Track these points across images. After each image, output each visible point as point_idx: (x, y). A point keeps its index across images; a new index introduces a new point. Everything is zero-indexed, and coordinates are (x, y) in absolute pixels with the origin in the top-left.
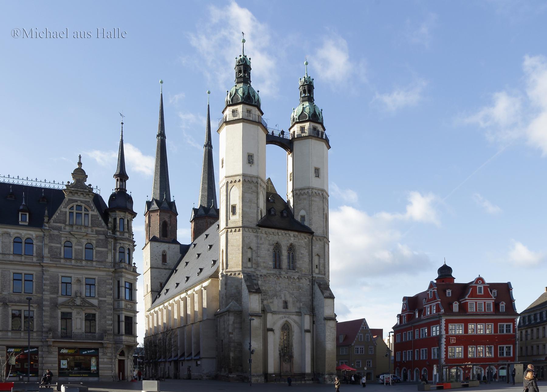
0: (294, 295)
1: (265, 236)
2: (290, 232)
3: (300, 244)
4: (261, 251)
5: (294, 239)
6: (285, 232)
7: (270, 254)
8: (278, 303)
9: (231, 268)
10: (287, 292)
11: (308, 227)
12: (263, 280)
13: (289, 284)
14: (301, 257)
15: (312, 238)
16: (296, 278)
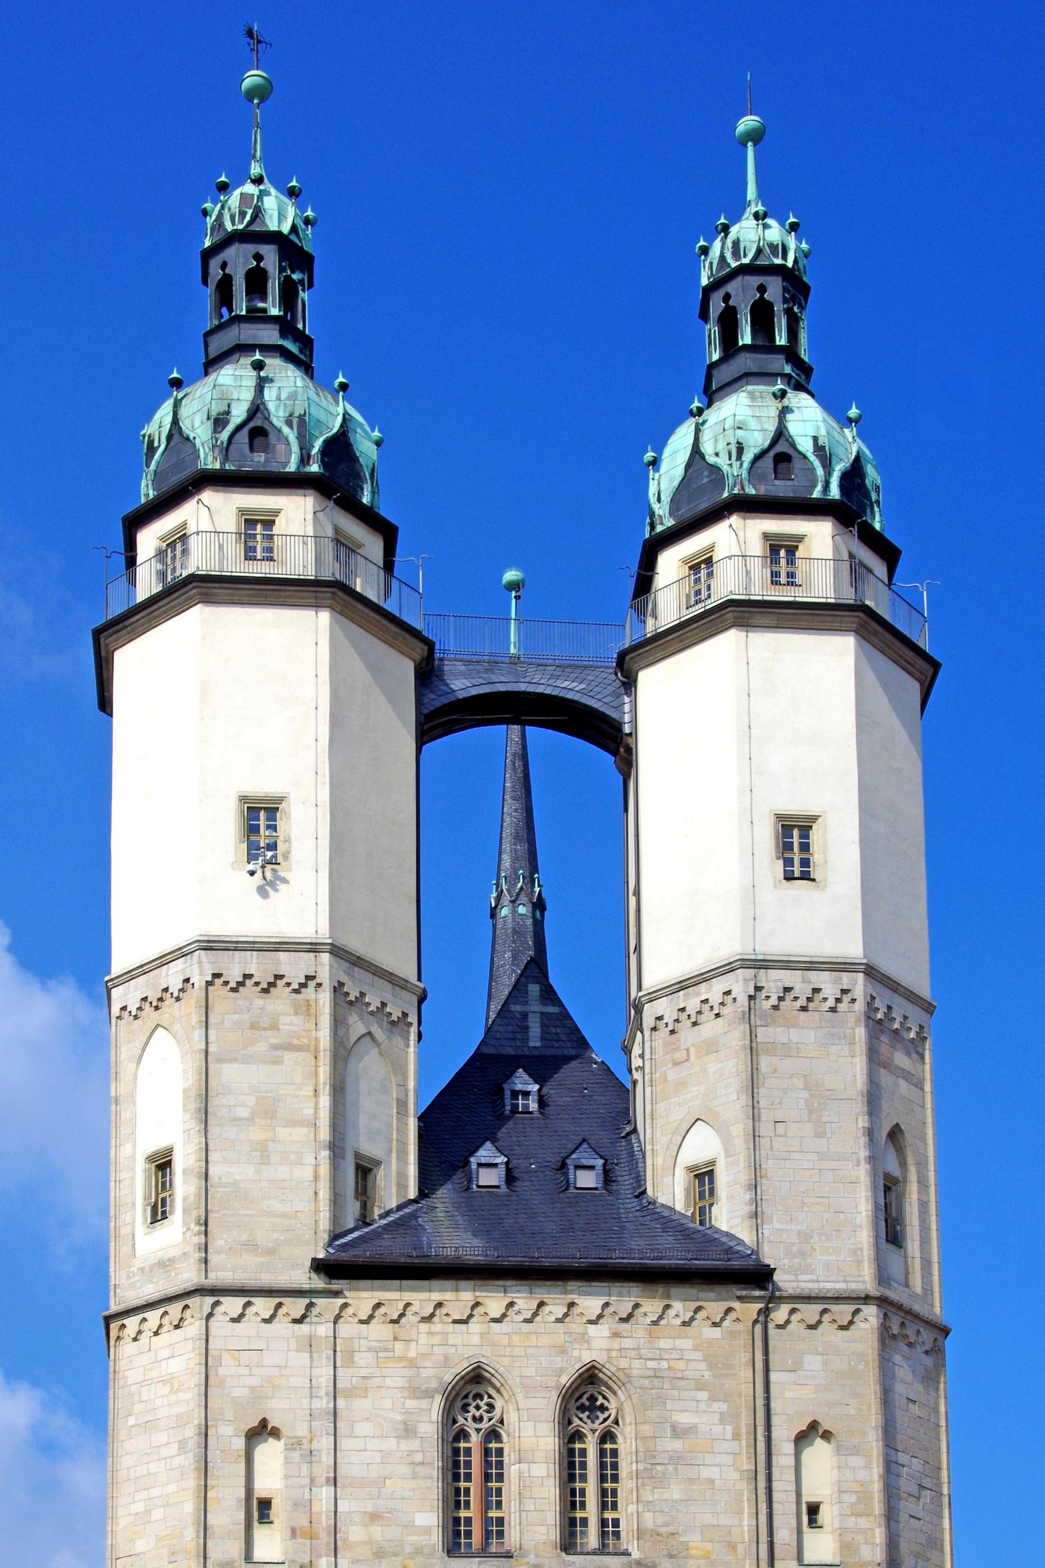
3: (664, 1364)
5: (616, 1335)
7: (419, 1458)
11: (733, 1237)
14: (676, 1459)
15: (765, 1312)
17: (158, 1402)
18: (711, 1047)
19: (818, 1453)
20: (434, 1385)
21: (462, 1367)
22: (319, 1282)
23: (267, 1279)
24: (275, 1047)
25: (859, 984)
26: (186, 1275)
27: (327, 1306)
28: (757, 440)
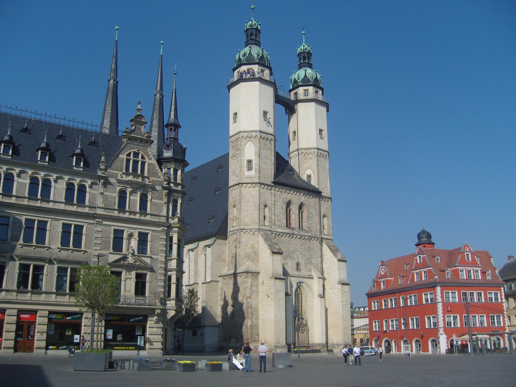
0: (306, 256)
1: (279, 193)
4: (276, 209)
7: (284, 213)
8: (292, 264)
9: (245, 225)
10: (299, 253)
11: (315, 186)
12: (278, 239)
13: (301, 244)
16: (307, 238)
17: (250, 198)
18: (311, 159)
19: (325, 219)
20: (285, 202)
21: (288, 200)
22: (273, 184)
23: (266, 183)
24: (267, 148)
26: (256, 180)
27: (273, 188)
28: (314, 77)
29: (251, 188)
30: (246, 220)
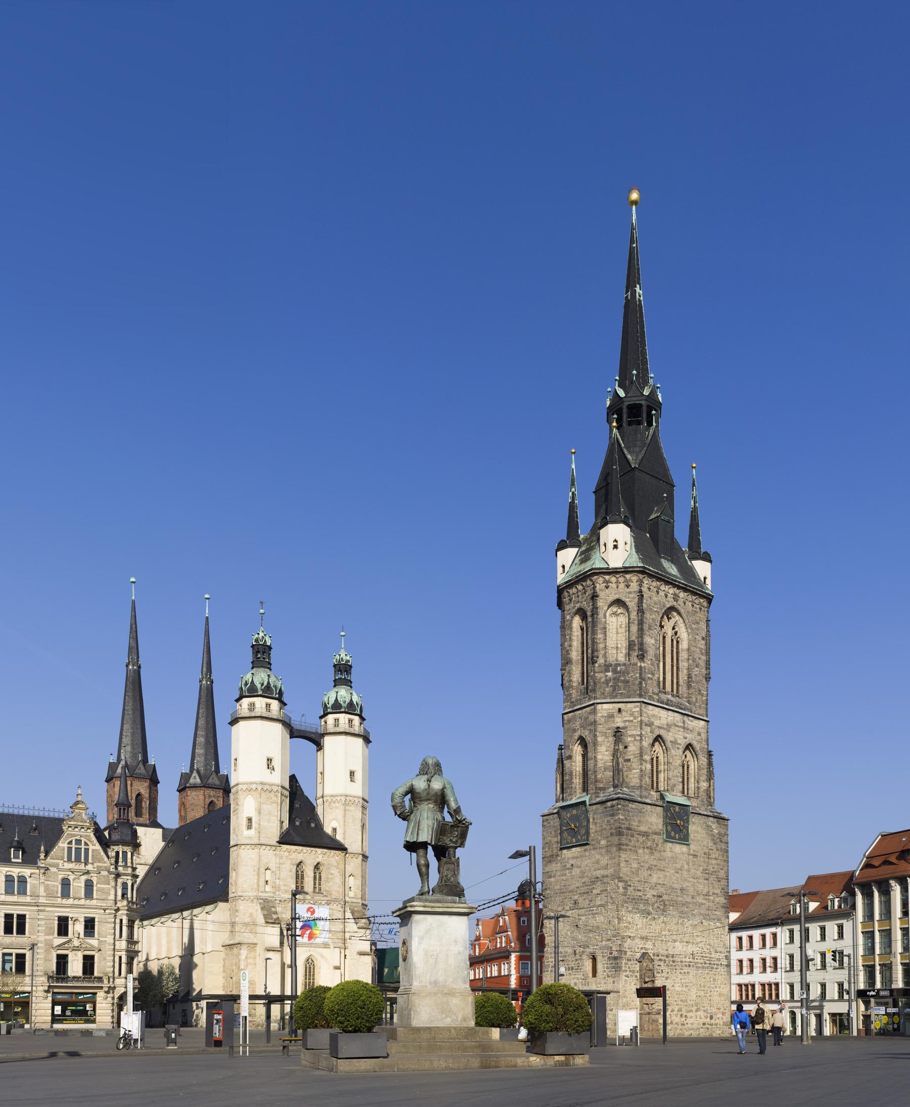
1: (287, 854)
2: (317, 849)
4: (281, 873)
6: (312, 849)
12: (283, 906)
14: (331, 879)
18: (337, 808)
22: (278, 845)
23: (269, 843)
25: (361, 801)
29: (250, 850)
30: (244, 886)
